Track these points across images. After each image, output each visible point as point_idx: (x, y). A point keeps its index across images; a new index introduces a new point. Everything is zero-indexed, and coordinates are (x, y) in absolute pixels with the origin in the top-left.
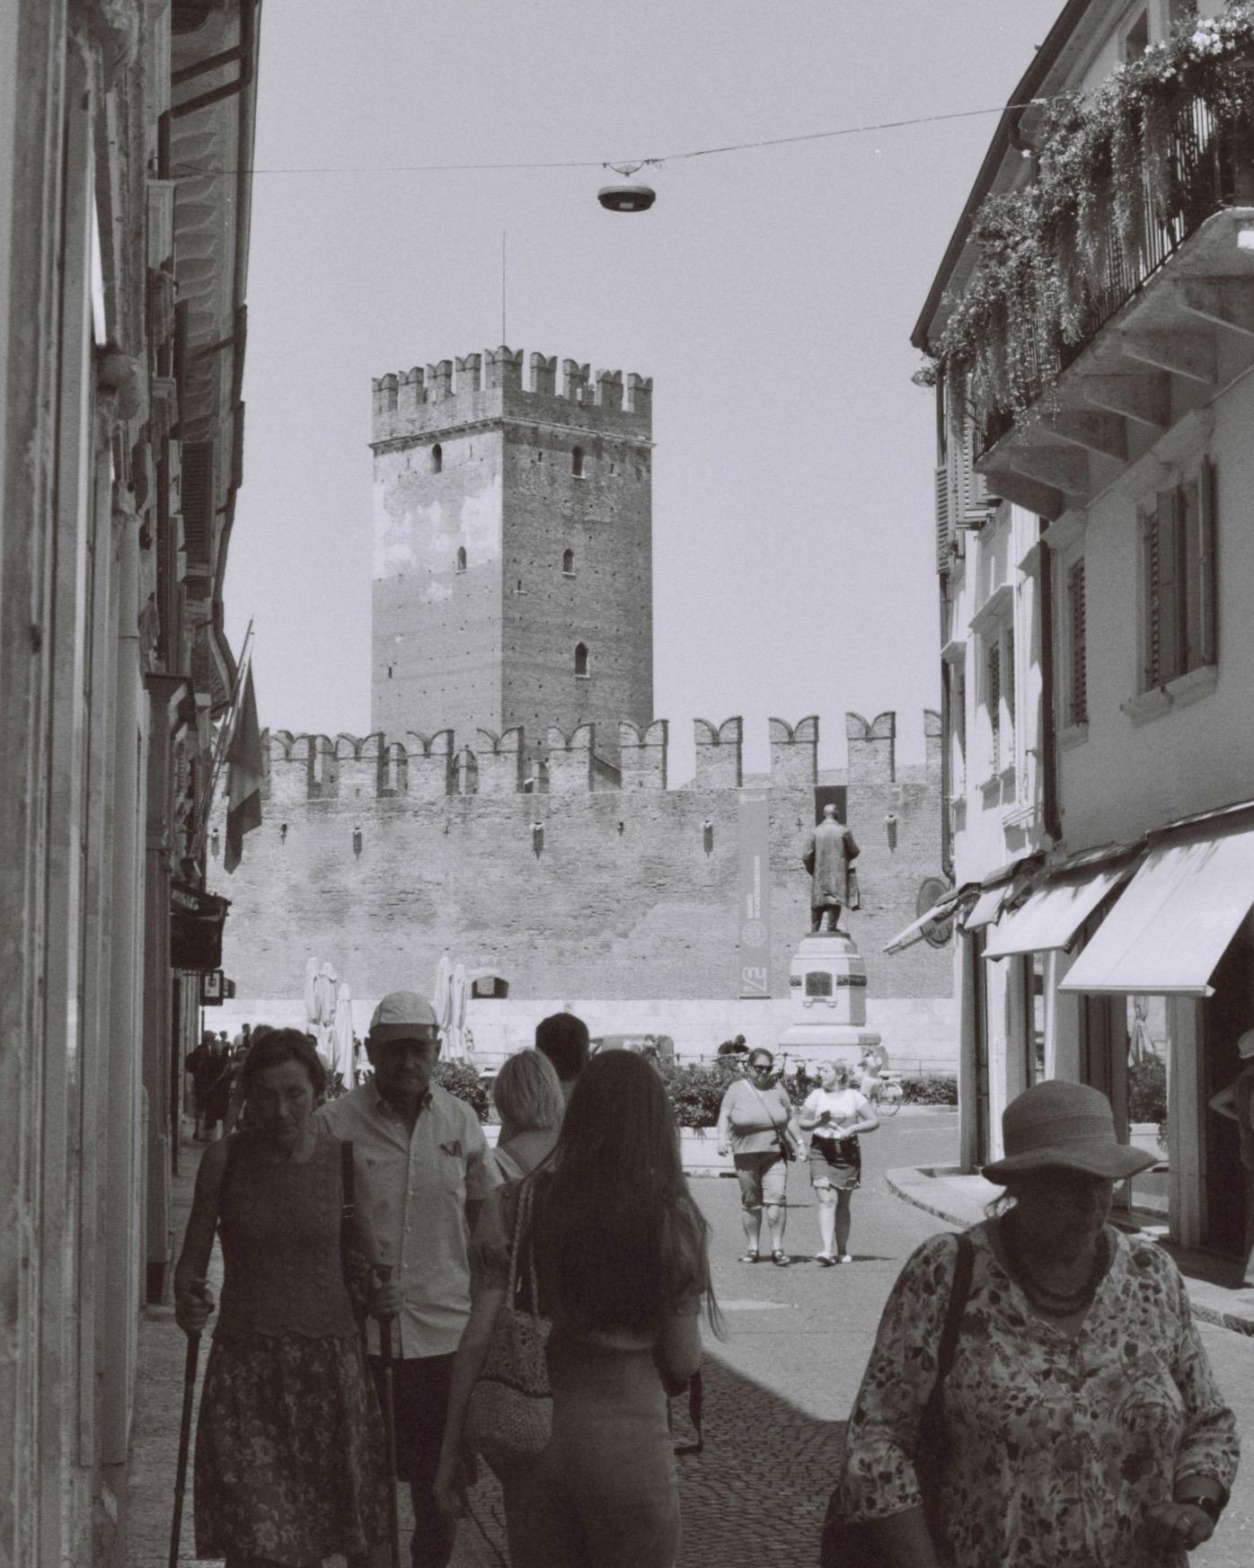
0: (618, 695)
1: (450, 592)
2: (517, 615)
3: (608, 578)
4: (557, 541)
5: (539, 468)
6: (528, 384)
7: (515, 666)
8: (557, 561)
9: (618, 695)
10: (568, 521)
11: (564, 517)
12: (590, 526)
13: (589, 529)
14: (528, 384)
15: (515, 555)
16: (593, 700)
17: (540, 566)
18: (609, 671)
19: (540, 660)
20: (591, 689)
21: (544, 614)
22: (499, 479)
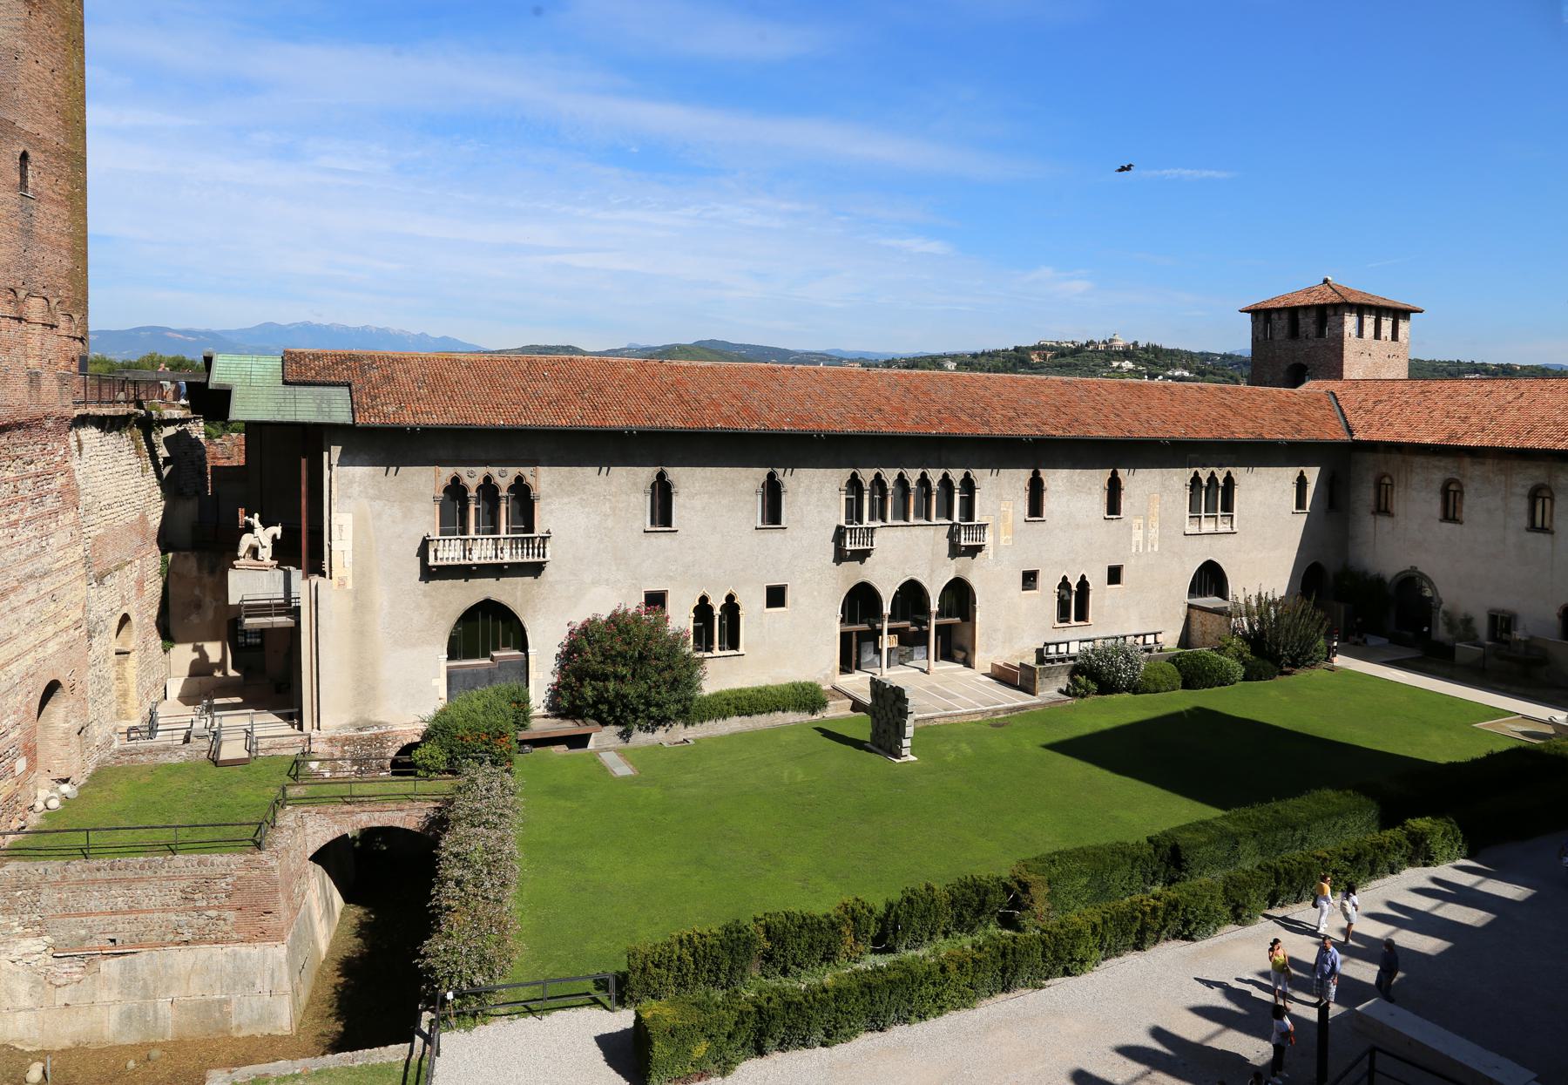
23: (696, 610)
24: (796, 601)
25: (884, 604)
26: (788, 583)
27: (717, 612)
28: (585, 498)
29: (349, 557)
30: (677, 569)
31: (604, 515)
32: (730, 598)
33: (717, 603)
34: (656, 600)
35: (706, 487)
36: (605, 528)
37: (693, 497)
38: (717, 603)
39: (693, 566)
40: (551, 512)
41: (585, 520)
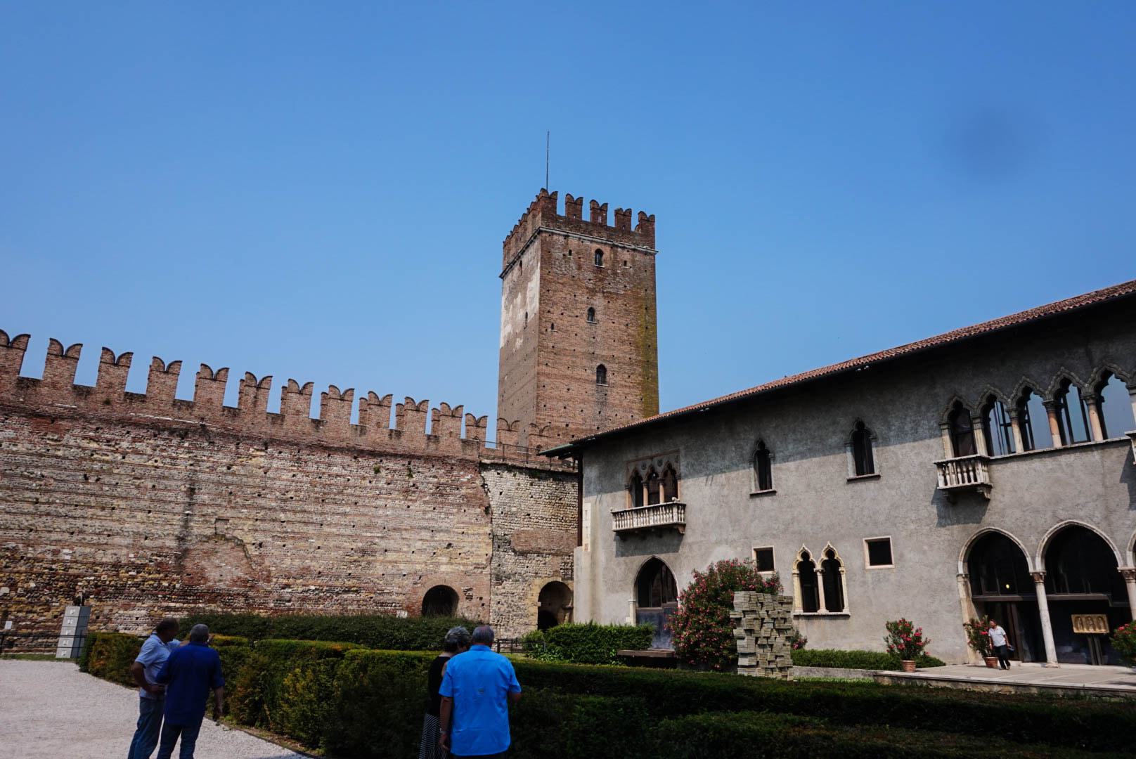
0: (630, 398)
1: (522, 341)
2: (551, 345)
3: (623, 327)
4: (582, 303)
5: (570, 259)
6: (561, 210)
7: (548, 375)
8: (582, 314)
9: (630, 398)
10: (592, 292)
11: (587, 288)
12: (608, 296)
13: (608, 297)
14: (561, 210)
15: (548, 309)
16: (610, 399)
17: (570, 316)
18: (623, 383)
19: (569, 372)
20: (609, 393)
21: (572, 345)
22: (539, 264)
23: (800, 566)
24: (902, 556)
25: (1029, 560)
26: (890, 537)
27: (818, 567)
28: (708, 473)
29: (589, 529)
30: (779, 527)
31: (722, 485)
32: (830, 553)
33: (818, 560)
34: (765, 559)
35: (798, 448)
36: (722, 496)
37: (788, 459)
38: (818, 560)
39: (792, 524)
40: (687, 488)
41: (709, 491)
